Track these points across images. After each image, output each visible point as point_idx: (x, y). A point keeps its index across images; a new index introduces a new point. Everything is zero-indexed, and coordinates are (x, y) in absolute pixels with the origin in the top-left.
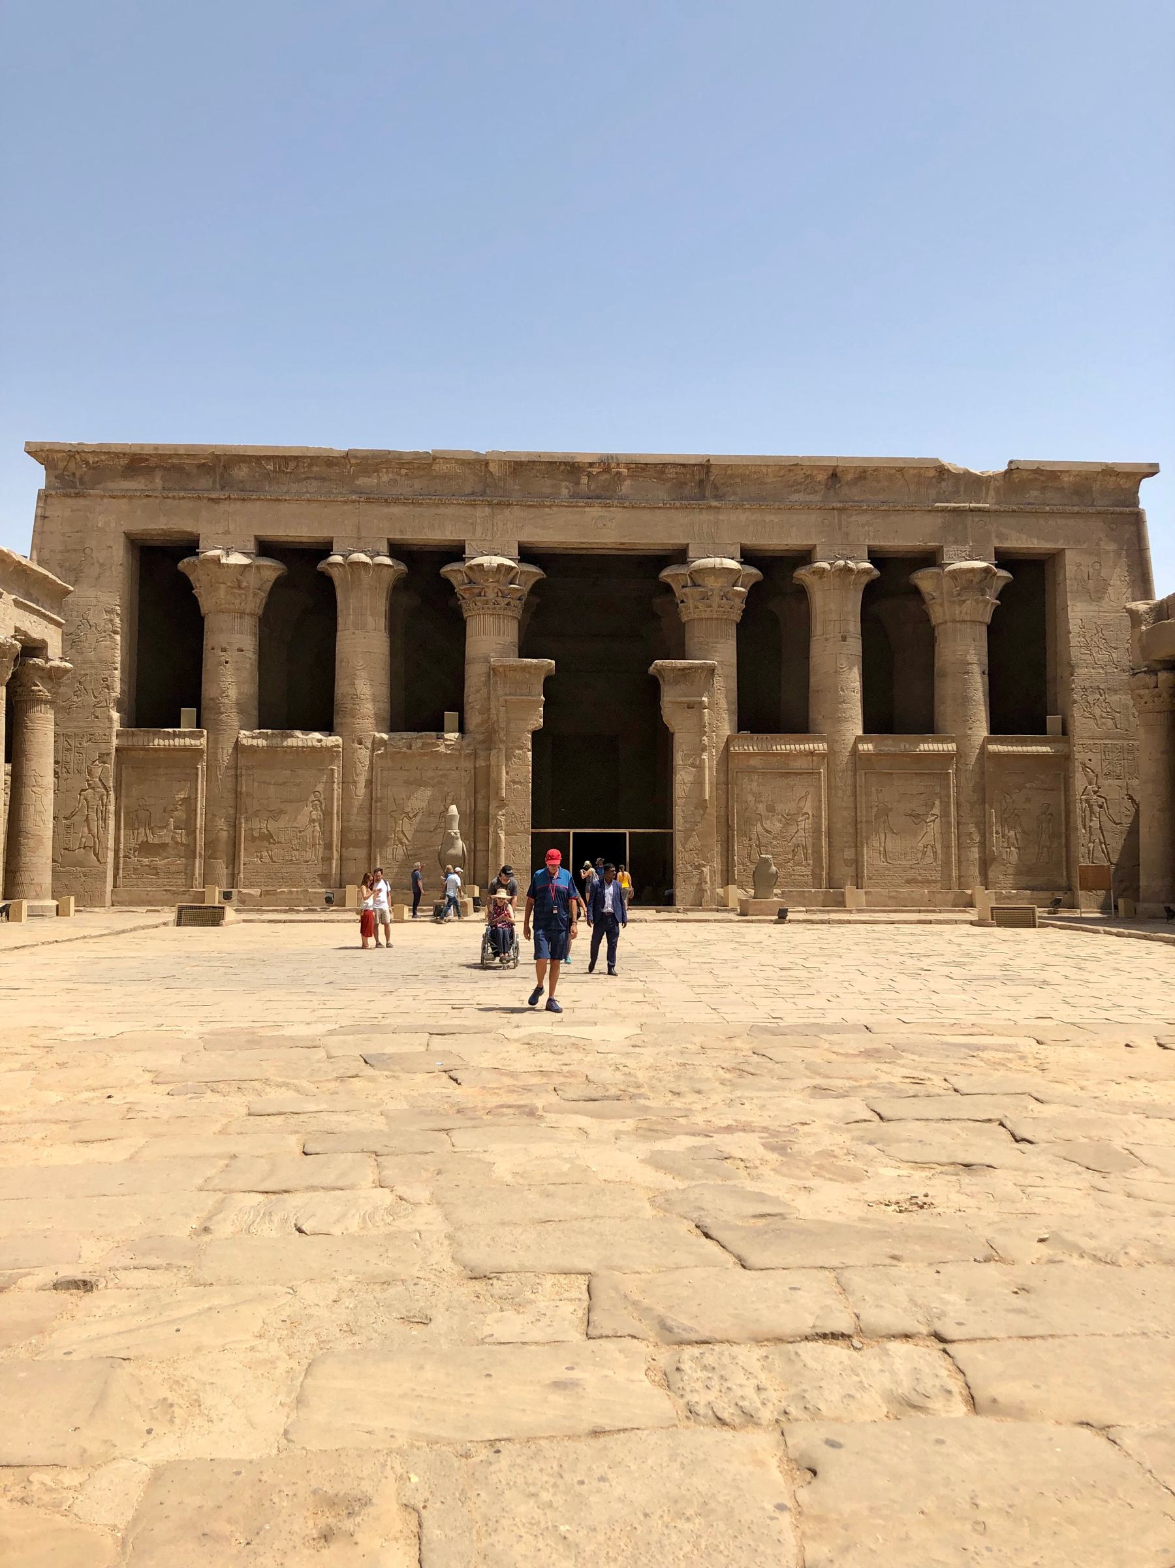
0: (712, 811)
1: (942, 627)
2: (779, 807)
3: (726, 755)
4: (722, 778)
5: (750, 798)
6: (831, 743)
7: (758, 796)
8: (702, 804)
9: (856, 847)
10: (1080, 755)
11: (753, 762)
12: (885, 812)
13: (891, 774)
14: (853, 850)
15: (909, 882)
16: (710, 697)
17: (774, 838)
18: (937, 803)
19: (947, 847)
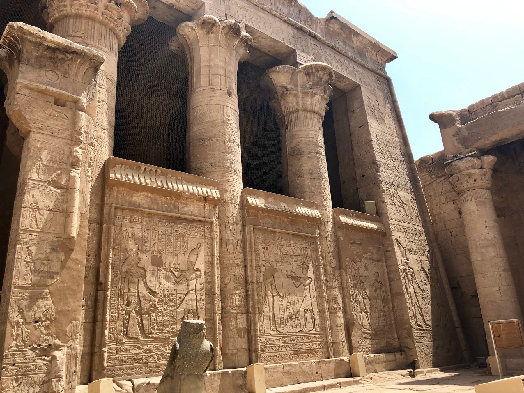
0: (80, 255)
1: (293, 116)
2: (168, 260)
3: (103, 183)
4: (95, 216)
5: (131, 245)
6: (223, 191)
7: (141, 243)
8: (65, 245)
9: (248, 312)
10: (395, 234)
11: (139, 198)
12: (271, 273)
13: (274, 232)
14: (244, 316)
15: (296, 353)
16: (90, 100)
17: (160, 301)
18: (311, 267)
19: (322, 312)
